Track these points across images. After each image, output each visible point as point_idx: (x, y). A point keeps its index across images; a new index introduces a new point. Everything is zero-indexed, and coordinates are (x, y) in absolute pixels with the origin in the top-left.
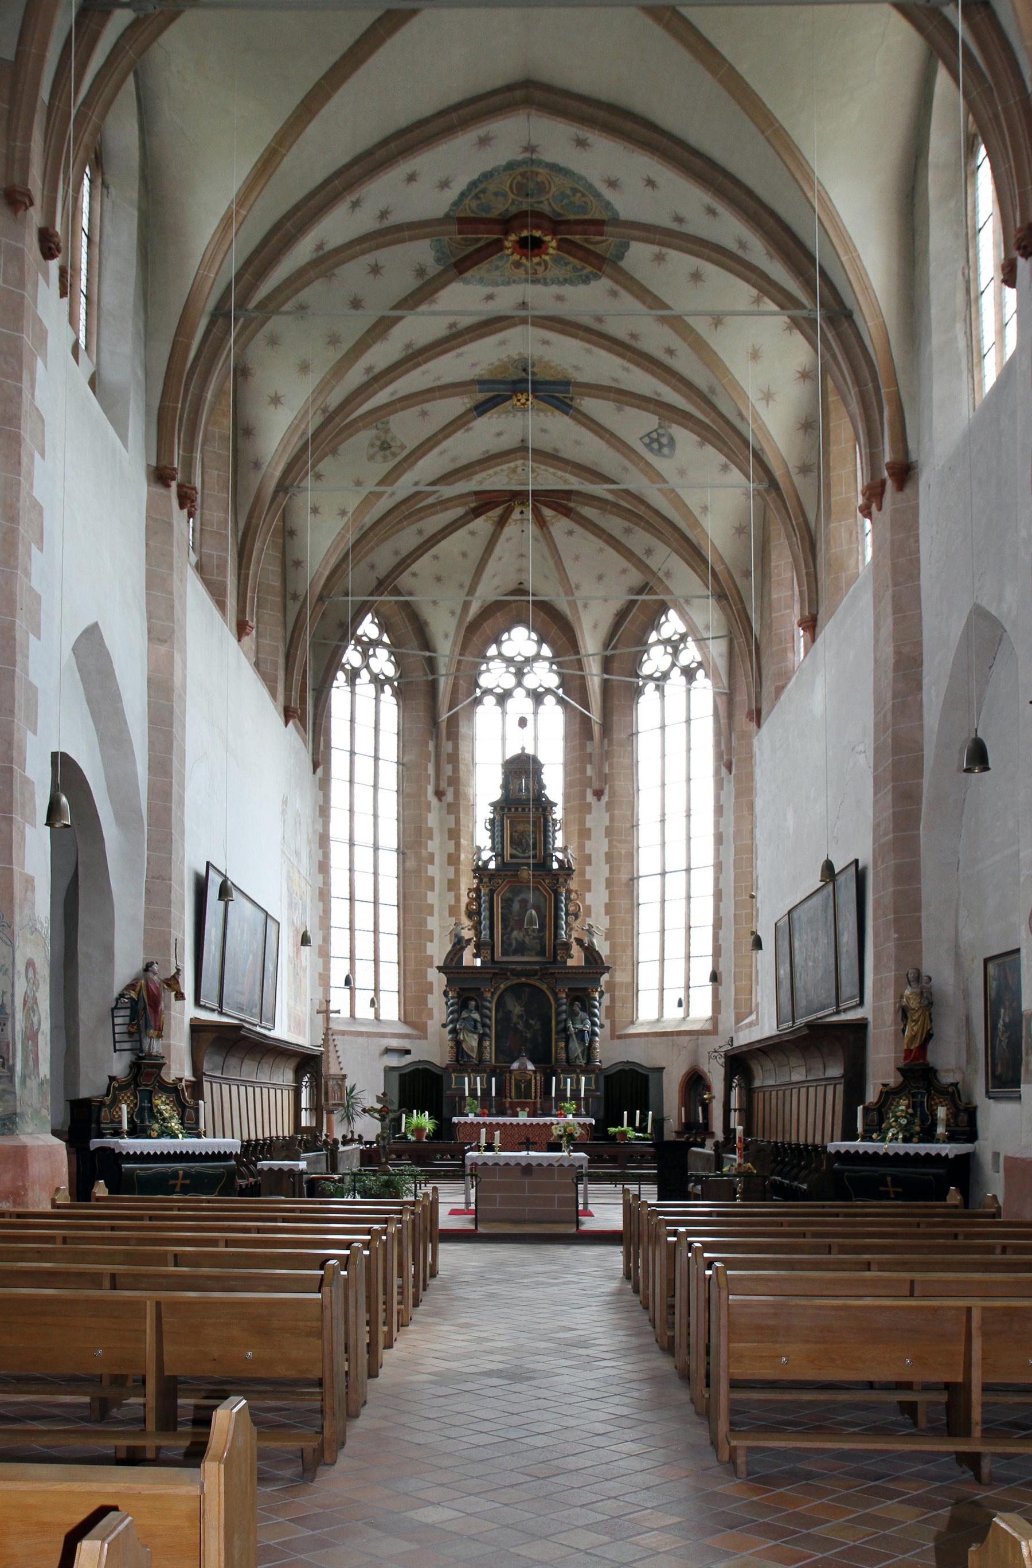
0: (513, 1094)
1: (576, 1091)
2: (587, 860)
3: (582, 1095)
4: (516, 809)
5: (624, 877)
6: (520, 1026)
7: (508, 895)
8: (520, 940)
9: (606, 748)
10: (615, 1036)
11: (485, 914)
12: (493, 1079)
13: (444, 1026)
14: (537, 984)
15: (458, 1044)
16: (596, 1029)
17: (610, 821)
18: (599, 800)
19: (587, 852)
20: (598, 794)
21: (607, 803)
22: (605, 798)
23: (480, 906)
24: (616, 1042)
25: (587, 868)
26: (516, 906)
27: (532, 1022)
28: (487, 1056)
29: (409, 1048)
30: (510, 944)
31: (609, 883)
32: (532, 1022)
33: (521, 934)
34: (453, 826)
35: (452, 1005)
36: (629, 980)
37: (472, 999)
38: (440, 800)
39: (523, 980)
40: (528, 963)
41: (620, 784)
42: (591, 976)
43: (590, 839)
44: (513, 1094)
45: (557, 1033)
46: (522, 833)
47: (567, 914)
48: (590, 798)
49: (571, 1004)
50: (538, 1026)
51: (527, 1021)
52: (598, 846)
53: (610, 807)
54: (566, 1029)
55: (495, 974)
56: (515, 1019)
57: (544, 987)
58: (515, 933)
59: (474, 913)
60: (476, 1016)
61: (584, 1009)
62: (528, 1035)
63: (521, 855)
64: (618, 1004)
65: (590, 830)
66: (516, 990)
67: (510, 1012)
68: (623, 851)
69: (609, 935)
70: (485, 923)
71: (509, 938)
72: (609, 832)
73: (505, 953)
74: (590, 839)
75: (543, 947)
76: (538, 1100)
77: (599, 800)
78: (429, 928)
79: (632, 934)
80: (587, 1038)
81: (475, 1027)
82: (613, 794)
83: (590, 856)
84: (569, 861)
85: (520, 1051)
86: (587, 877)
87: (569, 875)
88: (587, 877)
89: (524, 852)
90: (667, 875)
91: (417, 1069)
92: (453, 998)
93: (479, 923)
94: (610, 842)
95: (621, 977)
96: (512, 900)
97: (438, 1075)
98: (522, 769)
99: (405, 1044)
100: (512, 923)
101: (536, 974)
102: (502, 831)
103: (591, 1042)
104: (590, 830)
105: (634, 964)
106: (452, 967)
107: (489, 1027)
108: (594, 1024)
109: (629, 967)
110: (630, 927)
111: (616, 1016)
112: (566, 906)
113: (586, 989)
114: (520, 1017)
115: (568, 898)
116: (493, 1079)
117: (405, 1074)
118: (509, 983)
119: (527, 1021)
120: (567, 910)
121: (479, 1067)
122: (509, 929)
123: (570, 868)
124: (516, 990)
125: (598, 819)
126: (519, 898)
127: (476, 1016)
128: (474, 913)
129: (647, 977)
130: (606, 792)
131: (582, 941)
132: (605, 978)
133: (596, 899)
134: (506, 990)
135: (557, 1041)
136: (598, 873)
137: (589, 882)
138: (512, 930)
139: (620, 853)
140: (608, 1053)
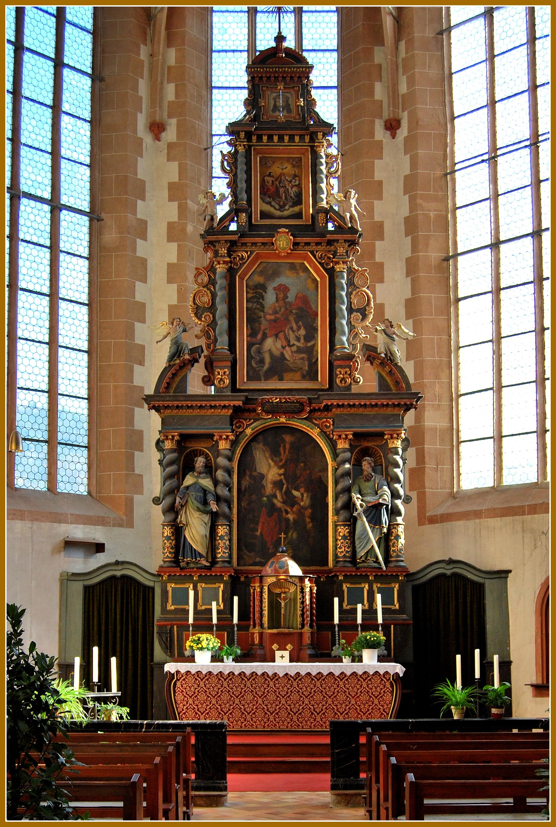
0: (265, 620)
1: (370, 613)
2: (378, 231)
3: (380, 621)
4: (270, 138)
5: (434, 255)
6: (278, 502)
7: (259, 279)
8: (277, 353)
9: (403, 53)
10: (425, 518)
11: (222, 308)
12: (236, 599)
13: (157, 501)
14: (304, 426)
15: (178, 531)
16: (398, 502)
17: (412, 169)
18: (394, 136)
19: (377, 218)
20: (392, 126)
21: (407, 140)
22: (403, 132)
23: (214, 296)
24: (428, 528)
25: (378, 243)
26: (270, 298)
27: (296, 493)
28: (221, 554)
29: (101, 541)
30: (262, 361)
31: (411, 267)
32: (296, 493)
33: (279, 345)
34: (177, 180)
35: (171, 464)
36: (445, 424)
37: (201, 453)
38: (157, 138)
39: (283, 420)
40: (290, 391)
41: (425, 108)
42: (389, 411)
43: (380, 198)
44: (265, 620)
45: (337, 512)
46: (279, 178)
47: (350, 310)
48: (380, 133)
49: (357, 464)
50: (306, 501)
51: (288, 493)
52: (392, 208)
53: (410, 145)
54: (349, 506)
55: (236, 409)
56: (269, 489)
57: (315, 433)
58: (269, 343)
59: (205, 309)
60: (207, 483)
61: (377, 467)
62: (291, 517)
63: (278, 213)
64: (430, 465)
65: (380, 183)
66: (271, 437)
67: (262, 477)
68: (432, 214)
69: (413, 348)
70: (223, 324)
71: (259, 352)
72: (410, 184)
73: (253, 376)
74: (380, 198)
75: (313, 365)
76: (307, 628)
77: (394, 136)
78: (138, 341)
79: (449, 349)
80: (385, 518)
81: (205, 503)
82: (414, 124)
83: (380, 225)
84: (352, 217)
85: (278, 543)
86: (378, 259)
87: (353, 243)
88: (378, 259)
89: (282, 208)
90: (502, 247)
91: (113, 577)
92: (172, 451)
93: (213, 324)
94: (412, 200)
95: (432, 419)
96: (263, 287)
97: (145, 587)
98: (277, 71)
99: (96, 534)
100: (264, 324)
101: (302, 411)
102: (248, 172)
103: (392, 526)
104: (380, 183)
105: (452, 398)
106: (168, 395)
107: (229, 503)
108: (395, 495)
109: (445, 403)
110: (445, 337)
111: (427, 484)
112: (349, 295)
113: (381, 435)
114: (278, 484)
115: (350, 283)
116: (236, 599)
117: (93, 586)
118: (258, 425)
119: (288, 493)
120: (350, 303)
121: (209, 571)
122: (259, 336)
123: (353, 230)
124: (271, 437)
125: (391, 165)
126: (275, 284)
127: (207, 483)
128: (205, 309)
129: (474, 417)
130: (405, 124)
131: (374, 349)
132: (409, 418)
133: (391, 293)
134: (254, 438)
135: (336, 526)
136: (391, 251)
137: (381, 266)
138: (265, 337)
139: (427, 217)
140: (419, 547)
